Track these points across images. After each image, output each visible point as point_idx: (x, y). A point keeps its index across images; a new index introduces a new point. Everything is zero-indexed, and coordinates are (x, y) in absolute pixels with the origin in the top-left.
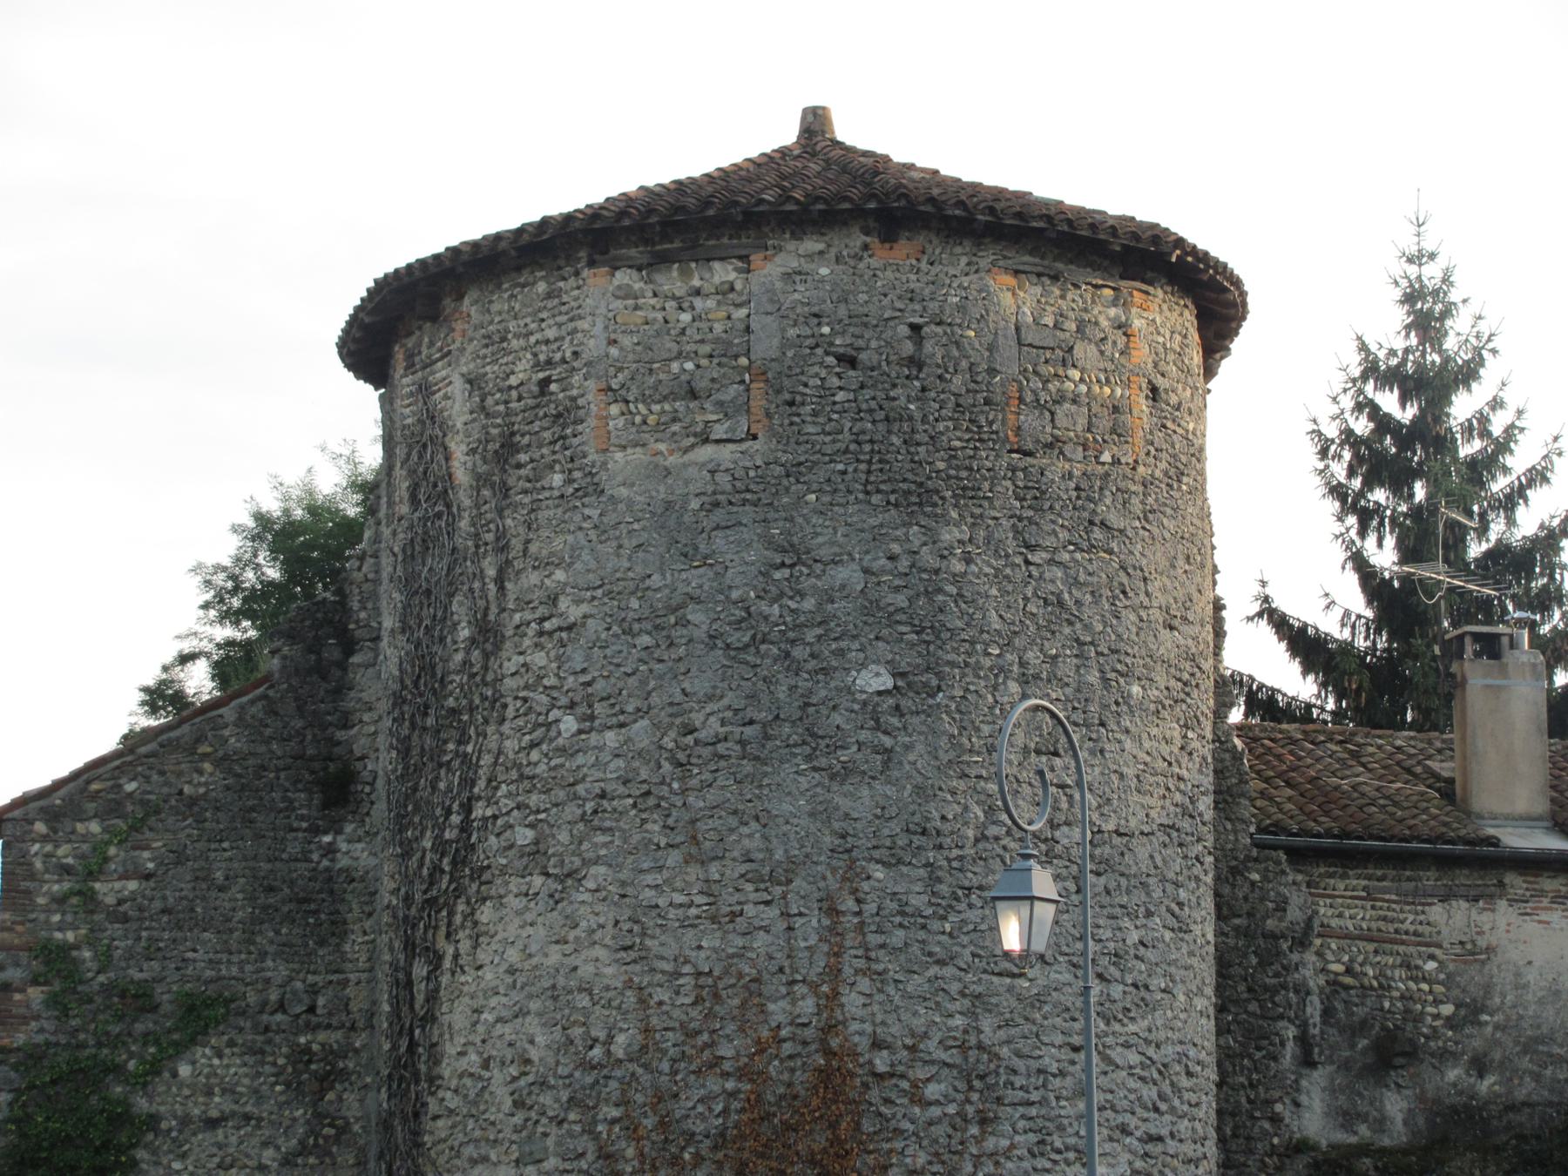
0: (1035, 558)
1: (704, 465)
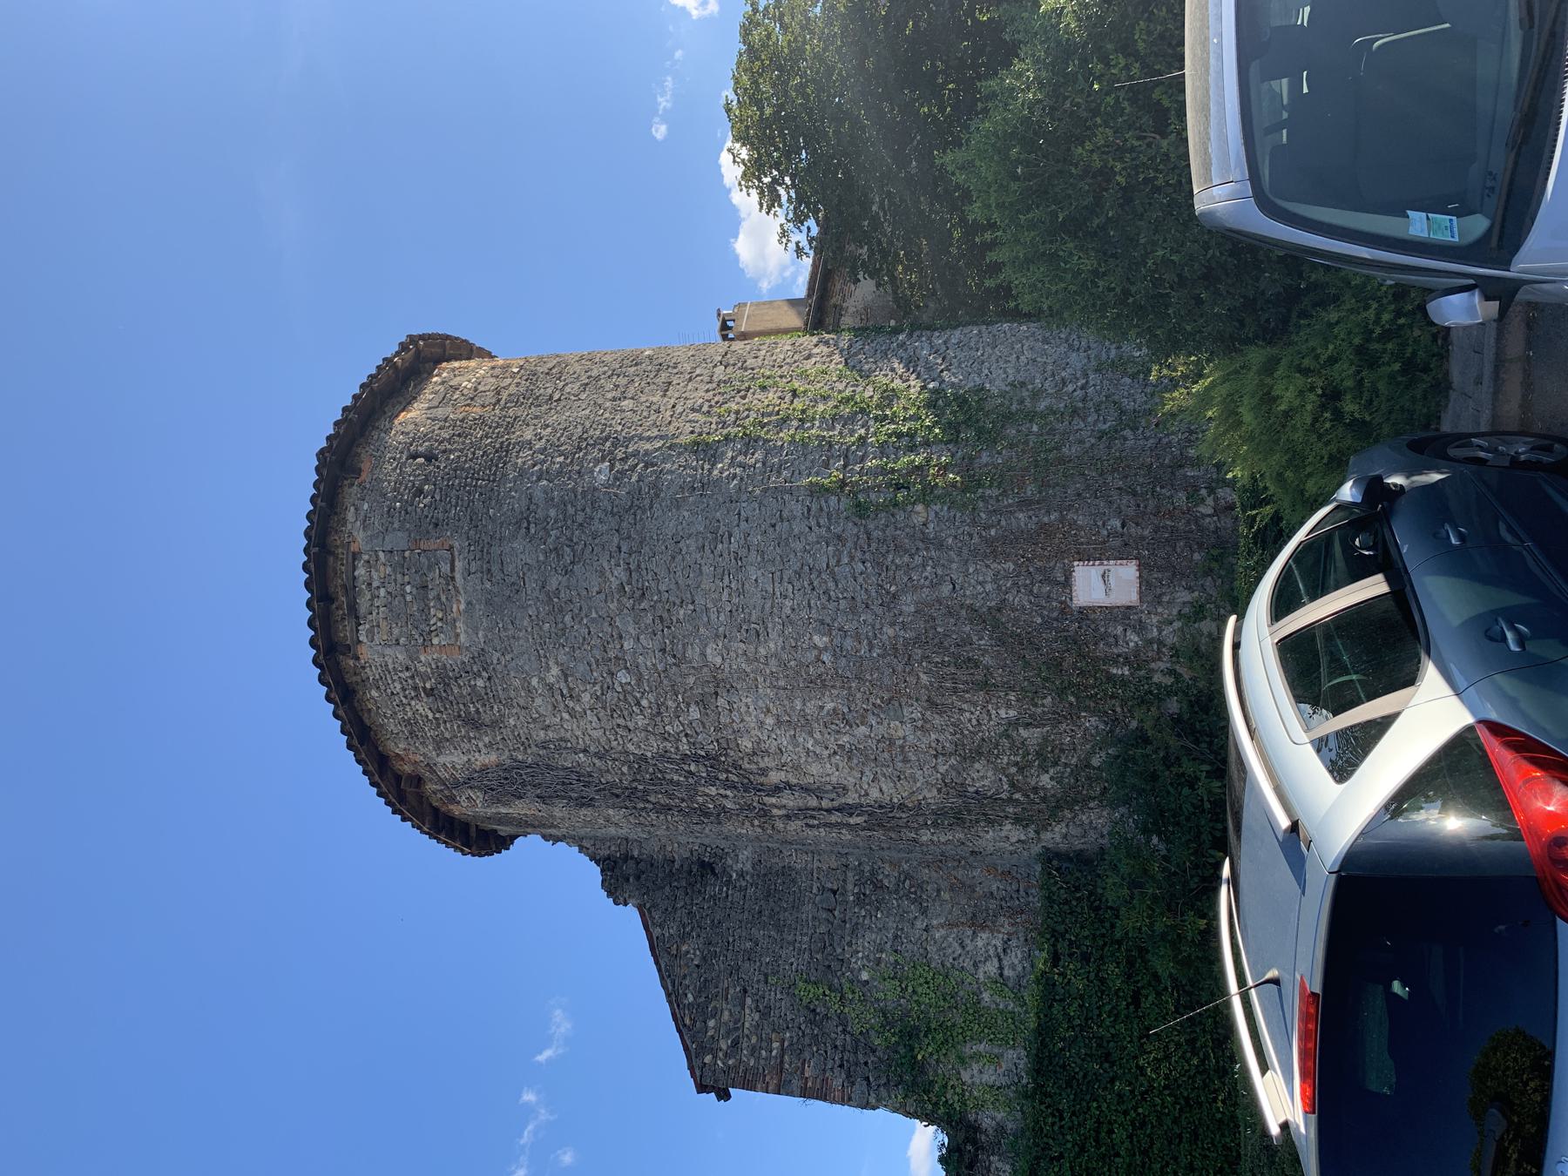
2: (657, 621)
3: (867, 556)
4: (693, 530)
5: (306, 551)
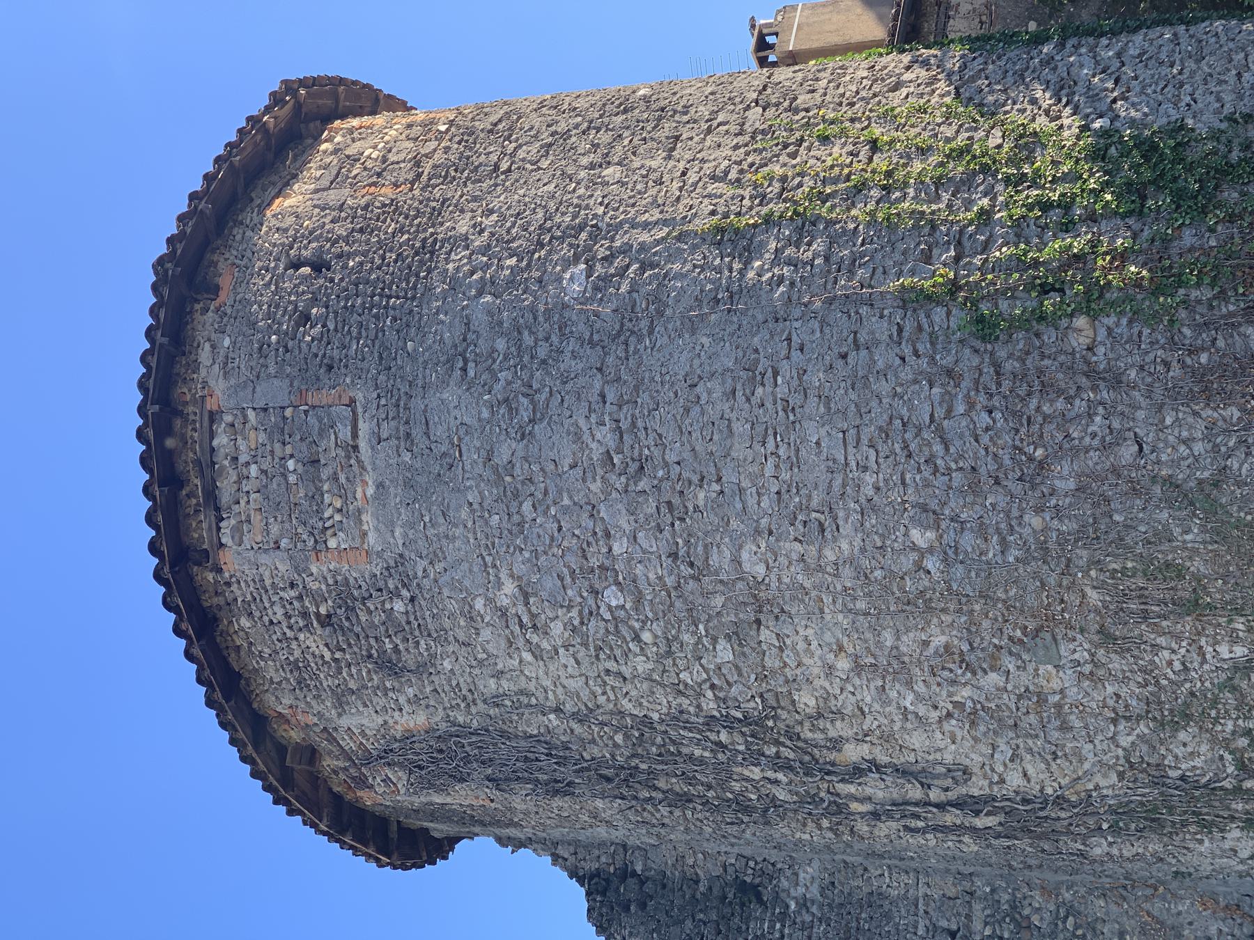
0: (504, 166)
1: (373, 448)
2: (664, 510)
3: (996, 401)
4: (717, 366)
5: (141, 410)
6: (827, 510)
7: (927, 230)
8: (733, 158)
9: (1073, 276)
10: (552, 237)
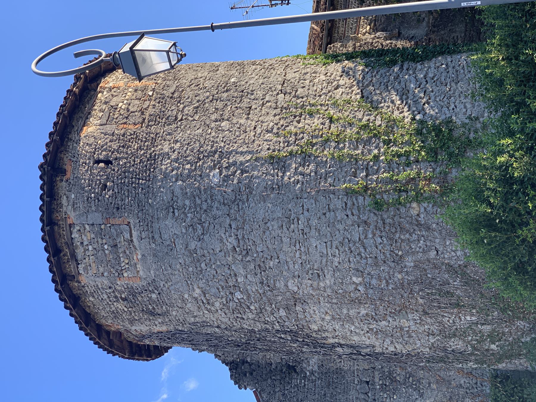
0: (180, 117)
1: (139, 242)
2: (257, 268)
3: (383, 234)
4: (275, 216)
5: (43, 230)
6: (320, 270)
7: (354, 162)
8: (275, 122)
9: (411, 187)
10: (204, 156)
